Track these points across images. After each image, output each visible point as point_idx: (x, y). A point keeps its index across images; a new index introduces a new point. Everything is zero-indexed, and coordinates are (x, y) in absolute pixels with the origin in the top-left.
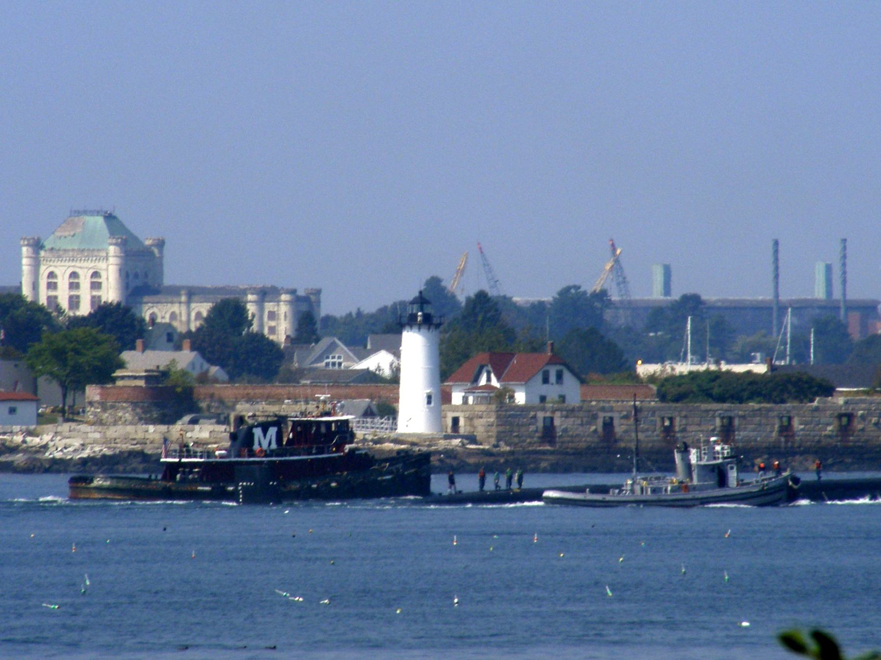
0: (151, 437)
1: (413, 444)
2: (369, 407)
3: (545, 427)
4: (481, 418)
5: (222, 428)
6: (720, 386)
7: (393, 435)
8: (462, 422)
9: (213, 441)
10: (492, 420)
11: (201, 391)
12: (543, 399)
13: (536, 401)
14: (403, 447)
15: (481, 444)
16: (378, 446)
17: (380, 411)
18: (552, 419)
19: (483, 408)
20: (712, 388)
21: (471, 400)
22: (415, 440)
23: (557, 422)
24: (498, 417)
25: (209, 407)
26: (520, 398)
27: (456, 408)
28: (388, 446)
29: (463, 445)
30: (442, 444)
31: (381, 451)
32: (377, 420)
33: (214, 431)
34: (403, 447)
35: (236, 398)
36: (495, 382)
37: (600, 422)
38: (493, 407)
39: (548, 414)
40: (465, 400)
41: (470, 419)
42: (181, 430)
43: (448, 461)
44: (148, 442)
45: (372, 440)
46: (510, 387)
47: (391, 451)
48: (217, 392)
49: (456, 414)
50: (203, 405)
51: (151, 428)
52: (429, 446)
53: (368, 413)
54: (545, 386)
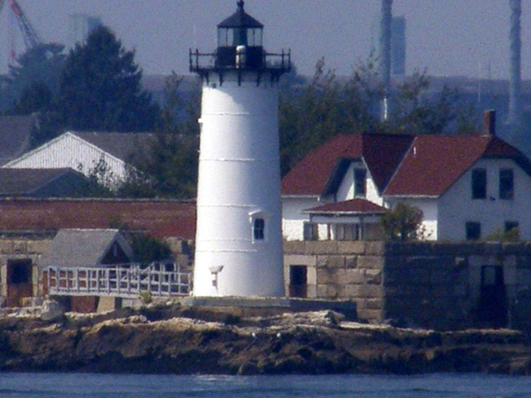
1: (232, 320)
2: (115, 243)
3: (484, 288)
4: (353, 265)
7: (184, 302)
8: (311, 276)
10: (374, 272)
12: (473, 230)
13: (459, 235)
14: (211, 325)
16: (158, 324)
17: (136, 252)
18: (499, 271)
19: (358, 247)
21: (323, 231)
22: (231, 310)
26: (429, 229)
27: (296, 247)
29: (334, 323)
30: (291, 320)
31: (168, 337)
32: (134, 269)
34: (211, 325)
36: (372, 194)
38: (379, 246)
39: (492, 261)
40: (310, 231)
41: (327, 270)
43: (319, 353)
46: (413, 205)
47: (190, 334)
49: (299, 260)
52: (265, 324)
53: (114, 257)
54: (480, 202)
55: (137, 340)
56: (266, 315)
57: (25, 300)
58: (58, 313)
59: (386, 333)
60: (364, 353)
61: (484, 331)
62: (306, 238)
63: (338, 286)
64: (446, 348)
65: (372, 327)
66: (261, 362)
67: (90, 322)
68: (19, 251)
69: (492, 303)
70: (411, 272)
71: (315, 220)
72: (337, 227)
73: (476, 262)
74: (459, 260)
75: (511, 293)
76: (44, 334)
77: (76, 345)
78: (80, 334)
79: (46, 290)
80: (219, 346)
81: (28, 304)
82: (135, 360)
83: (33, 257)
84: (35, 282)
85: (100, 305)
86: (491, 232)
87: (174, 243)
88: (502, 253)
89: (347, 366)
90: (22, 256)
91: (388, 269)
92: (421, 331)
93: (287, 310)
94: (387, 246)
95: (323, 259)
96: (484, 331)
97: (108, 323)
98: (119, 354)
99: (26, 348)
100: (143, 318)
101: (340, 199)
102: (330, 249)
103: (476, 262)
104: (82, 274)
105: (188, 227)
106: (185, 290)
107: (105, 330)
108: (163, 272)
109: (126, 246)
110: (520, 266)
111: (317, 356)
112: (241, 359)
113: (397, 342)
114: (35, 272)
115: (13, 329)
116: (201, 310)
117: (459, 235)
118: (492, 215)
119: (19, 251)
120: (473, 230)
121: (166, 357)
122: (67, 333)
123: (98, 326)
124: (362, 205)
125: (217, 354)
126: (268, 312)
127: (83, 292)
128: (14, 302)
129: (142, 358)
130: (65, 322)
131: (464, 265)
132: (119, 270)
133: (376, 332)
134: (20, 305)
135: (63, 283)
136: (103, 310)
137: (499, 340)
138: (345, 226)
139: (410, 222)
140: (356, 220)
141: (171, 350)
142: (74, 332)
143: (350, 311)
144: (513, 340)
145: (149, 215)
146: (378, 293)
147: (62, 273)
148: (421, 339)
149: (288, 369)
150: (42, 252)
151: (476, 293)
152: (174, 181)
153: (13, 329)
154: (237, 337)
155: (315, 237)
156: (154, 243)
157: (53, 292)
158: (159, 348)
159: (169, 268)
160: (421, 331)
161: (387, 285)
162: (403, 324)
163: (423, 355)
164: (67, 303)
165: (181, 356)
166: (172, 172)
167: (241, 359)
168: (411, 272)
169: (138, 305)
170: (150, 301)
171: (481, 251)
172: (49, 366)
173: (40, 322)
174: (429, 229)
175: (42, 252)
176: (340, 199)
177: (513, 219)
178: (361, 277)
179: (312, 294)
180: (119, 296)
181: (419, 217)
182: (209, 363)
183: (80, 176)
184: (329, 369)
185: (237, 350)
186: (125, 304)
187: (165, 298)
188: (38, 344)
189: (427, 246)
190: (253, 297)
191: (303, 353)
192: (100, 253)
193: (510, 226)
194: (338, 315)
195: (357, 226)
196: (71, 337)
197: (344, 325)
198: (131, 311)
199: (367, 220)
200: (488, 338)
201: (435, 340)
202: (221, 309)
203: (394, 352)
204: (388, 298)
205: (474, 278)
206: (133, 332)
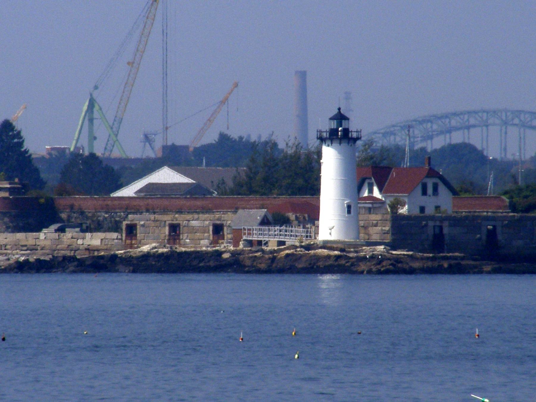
0: (42, 243)
5: (115, 235)
9: (105, 247)
17: (275, 220)
42: (72, 238)
44: (39, 248)
57: (220, 241)
81: (223, 243)
83: (224, 223)
109: (270, 217)
114: (225, 228)
119: (219, 219)
175: (229, 219)
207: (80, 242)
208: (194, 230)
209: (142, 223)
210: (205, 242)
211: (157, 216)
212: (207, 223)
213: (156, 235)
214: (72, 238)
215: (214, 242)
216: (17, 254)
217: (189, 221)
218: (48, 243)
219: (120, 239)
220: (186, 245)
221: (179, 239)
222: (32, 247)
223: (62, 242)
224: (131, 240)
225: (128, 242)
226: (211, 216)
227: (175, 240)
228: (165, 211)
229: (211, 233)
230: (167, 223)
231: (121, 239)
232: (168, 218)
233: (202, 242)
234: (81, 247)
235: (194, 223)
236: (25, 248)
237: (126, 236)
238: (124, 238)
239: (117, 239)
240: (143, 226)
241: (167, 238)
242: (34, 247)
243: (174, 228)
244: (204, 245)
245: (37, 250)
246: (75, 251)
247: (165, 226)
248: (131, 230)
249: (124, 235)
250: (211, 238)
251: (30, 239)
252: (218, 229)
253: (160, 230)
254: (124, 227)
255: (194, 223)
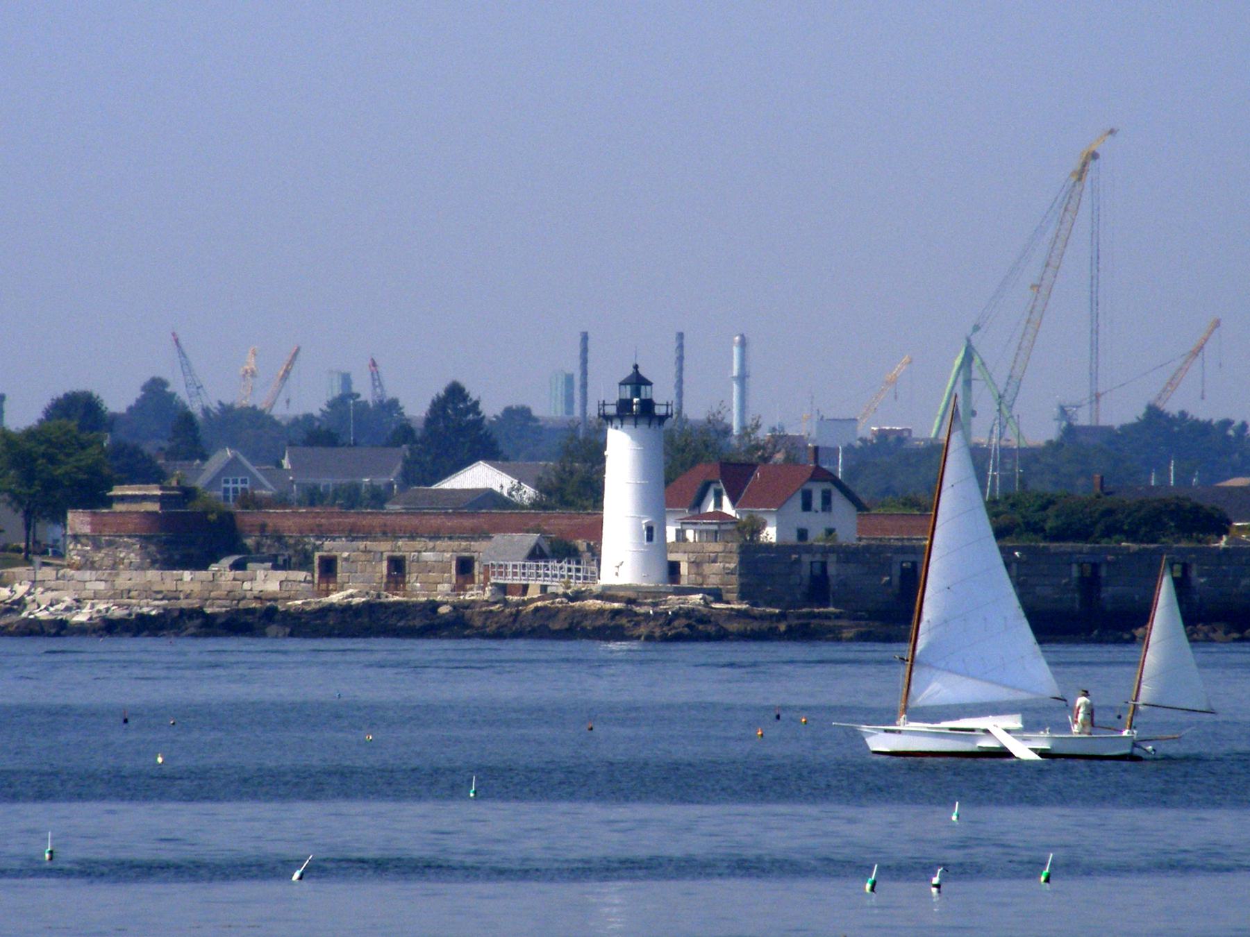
0: (186, 588)
1: (630, 601)
2: (537, 545)
3: (813, 578)
4: (715, 561)
5: (301, 575)
6: (1057, 516)
8: (684, 569)
10: (732, 566)
11: (248, 519)
12: (803, 534)
13: (792, 539)
14: (616, 605)
15: (728, 603)
17: (553, 551)
18: (824, 566)
19: (717, 547)
20: (1044, 521)
21: (690, 534)
23: (832, 570)
24: (741, 562)
25: (259, 545)
26: (770, 534)
28: (593, 604)
29: (707, 604)
30: (673, 602)
31: (585, 614)
32: (553, 563)
33: (287, 580)
34: (616, 605)
35: (301, 532)
36: (727, 507)
37: (896, 571)
38: (734, 546)
39: (818, 557)
40: (680, 535)
41: (696, 564)
42: (234, 579)
45: (565, 595)
47: (601, 612)
48: (270, 522)
50: (249, 542)
51: (187, 575)
53: (536, 554)
54: (806, 514)
55: (562, 616)
56: (654, 597)
57: (468, 586)
58: (500, 597)
59: (746, 610)
60: (733, 626)
61: (816, 610)
62: (677, 540)
63: (704, 577)
64: (795, 622)
65: (735, 606)
66: (658, 632)
67: (525, 603)
68: (465, 550)
69: (819, 588)
70: (758, 566)
71: (685, 527)
72: (701, 532)
73: (806, 558)
74: (794, 556)
75: (833, 581)
76: (491, 611)
77: (515, 621)
78: (518, 612)
79: (487, 579)
80: (624, 621)
81: (471, 589)
82: (555, 631)
83: (476, 555)
84: (476, 572)
85: (529, 591)
86: (816, 535)
87: (581, 544)
88: (826, 551)
89: (722, 636)
90: (466, 554)
91: (742, 562)
92: (769, 610)
93: (670, 594)
94: (741, 546)
95: (693, 557)
96: (816, 610)
97: (539, 604)
98: (547, 626)
99: (478, 622)
100: (565, 600)
101: (703, 511)
102: (698, 549)
103: (806, 558)
104: (515, 566)
105: (595, 532)
106: (593, 578)
107: (537, 609)
108: (573, 566)
109: (546, 547)
110: (838, 561)
111: (695, 629)
112: (643, 630)
113: (754, 618)
114: (476, 564)
115: (467, 608)
116: (606, 594)
117: (792, 539)
118: (816, 523)
119: (465, 550)
120: (803, 534)
121: (583, 629)
122: (507, 611)
123: (532, 606)
124: (720, 516)
125: (622, 627)
126: (656, 595)
127: (518, 581)
128: (459, 588)
129: (567, 630)
130: (506, 603)
131: (798, 561)
132: (542, 564)
133: (738, 610)
134: (465, 590)
135: (500, 574)
136: (533, 593)
137: (827, 616)
138: (707, 531)
139: (756, 528)
140: (715, 527)
141: (588, 624)
142: (514, 610)
143: (717, 595)
144: (838, 616)
145: (560, 522)
146: (734, 583)
147: (501, 566)
148: (772, 616)
149: (679, 638)
150: (482, 551)
151: (806, 581)
152: (571, 498)
153: (467, 608)
154: (636, 614)
155: (685, 540)
156: (566, 544)
157: (493, 580)
158: (578, 623)
159: (578, 563)
160: (769, 610)
161: (740, 575)
162: (755, 604)
163: (777, 627)
164: (503, 589)
165: (594, 628)
166: (578, 487)
167: (643, 630)
168: (758, 566)
169: (561, 590)
170: (569, 588)
171: (810, 550)
172: (498, 635)
173: (487, 603)
174: (770, 534)
175: (482, 551)
176: (703, 511)
177: (832, 526)
178: (722, 568)
179: (684, 582)
180: (547, 583)
181: (764, 525)
182: (617, 634)
183: (501, 495)
184: (708, 638)
185: (637, 624)
186: (550, 590)
187: (577, 585)
188: (486, 619)
189: (769, 546)
190: (645, 584)
191: (688, 626)
192: (526, 552)
193: (830, 532)
194: (711, 598)
195: (716, 532)
196: (511, 614)
197: (714, 606)
198: (556, 595)
199: (723, 527)
200: (819, 616)
201: (782, 617)
202: (622, 594)
203: (755, 625)
204: (742, 585)
205: (805, 571)
206: (558, 611)
207: (247, 586)
208: (426, 568)
209: (346, 554)
210: (445, 587)
211: (369, 544)
212: (448, 555)
213: (367, 575)
214: (234, 579)
215: (459, 588)
216: (148, 605)
217: (419, 552)
218: (197, 587)
219: (309, 582)
220: (417, 590)
221: (404, 583)
222: (171, 595)
223: (218, 587)
224: (328, 582)
225: (323, 586)
226: (455, 544)
227: (397, 583)
228: (367, 535)
229: (454, 571)
230: (386, 555)
231: (313, 582)
232: (385, 547)
233: (440, 587)
234: (249, 594)
235: (428, 556)
236: (160, 596)
237: (320, 577)
238: (316, 581)
239: (305, 581)
240: (346, 559)
241: (385, 580)
242: (174, 594)
243: (397, 566)
244: (444, 592)
245: (178, 599)
246: (239, 601)
247: (381, 560)
248: (329, 567)
249: (316, 575)
250: (454, 580)
251: (168, 581)
252: (465, 567)
253: (374, 567)
254: (316, 562)
255: (428, 556)
